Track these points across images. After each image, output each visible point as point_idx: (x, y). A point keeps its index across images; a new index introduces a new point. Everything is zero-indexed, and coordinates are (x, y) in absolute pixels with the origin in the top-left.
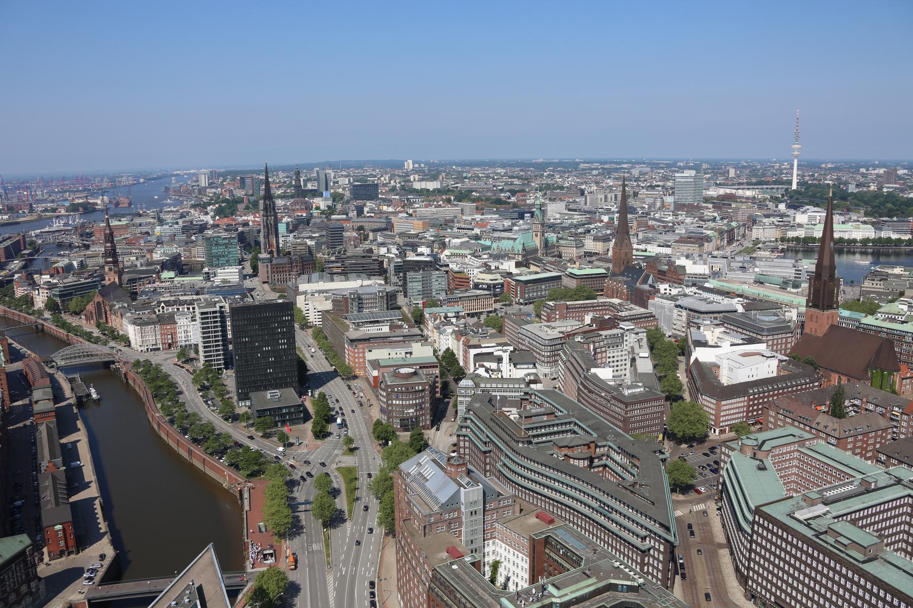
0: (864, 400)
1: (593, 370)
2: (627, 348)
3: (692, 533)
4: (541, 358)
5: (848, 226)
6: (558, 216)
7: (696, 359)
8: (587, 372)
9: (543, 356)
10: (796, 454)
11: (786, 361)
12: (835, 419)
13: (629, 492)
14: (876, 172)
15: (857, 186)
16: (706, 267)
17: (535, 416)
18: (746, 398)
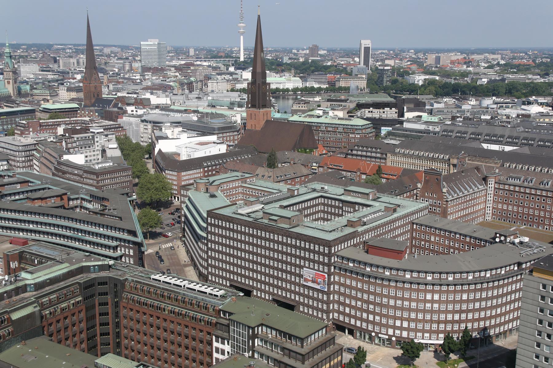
0: (292, 162)
1: (65, 157)
2: (98, 148)
3: (162, 260)
4: (16, 164)
5: (283, 79)
6: (32, 76)
7: (160, 150)
8: (60, 158)
9: (18, 161)
10: (240, 190)
11: (232, 146)
12: (269, 170)
13: (99, 216)
14: (304, 52)
15: (290, 59)
16: (168, 99)
17: (8, 185)
18: (202, 170)
